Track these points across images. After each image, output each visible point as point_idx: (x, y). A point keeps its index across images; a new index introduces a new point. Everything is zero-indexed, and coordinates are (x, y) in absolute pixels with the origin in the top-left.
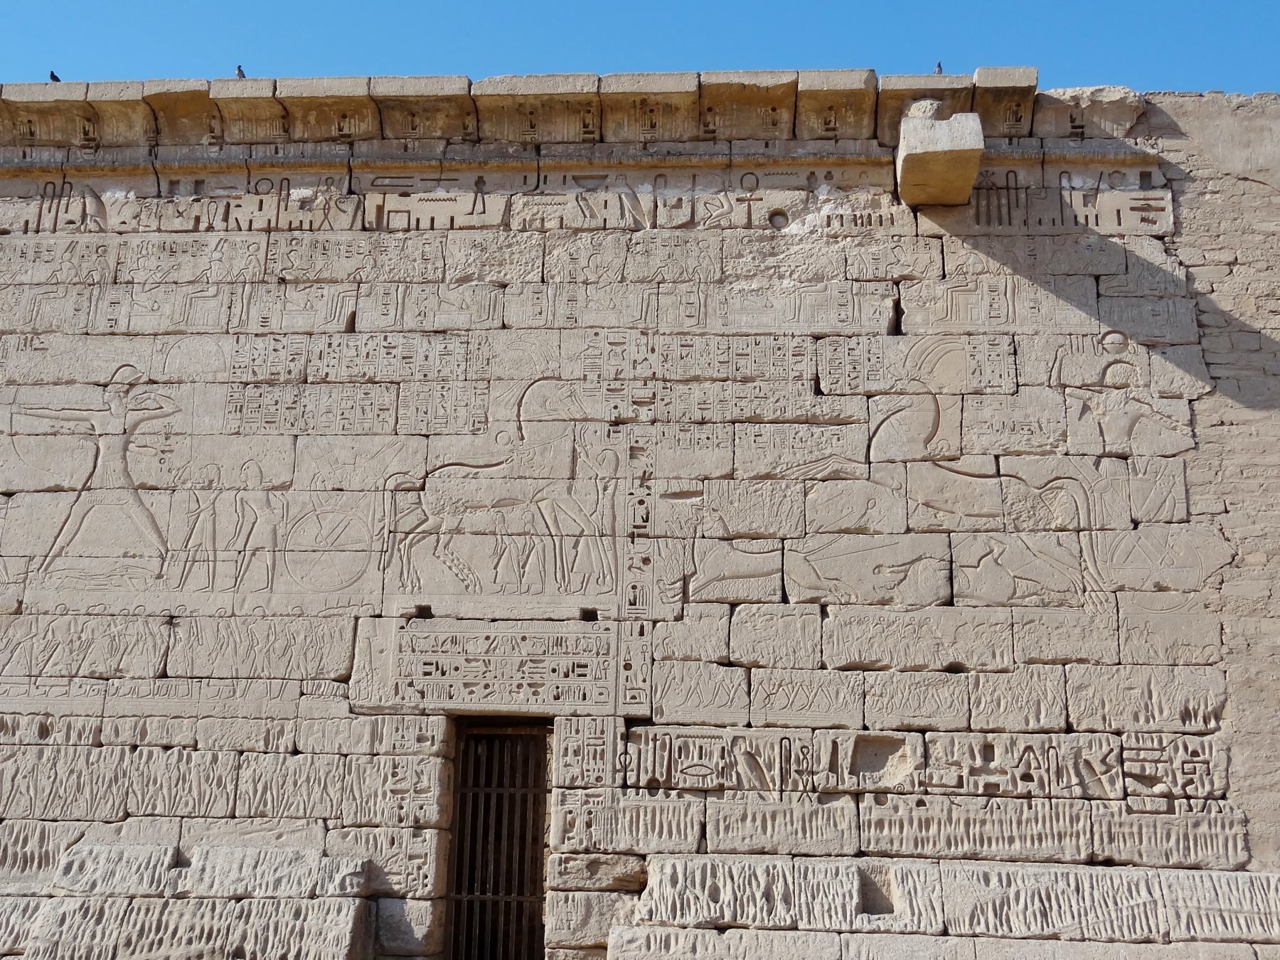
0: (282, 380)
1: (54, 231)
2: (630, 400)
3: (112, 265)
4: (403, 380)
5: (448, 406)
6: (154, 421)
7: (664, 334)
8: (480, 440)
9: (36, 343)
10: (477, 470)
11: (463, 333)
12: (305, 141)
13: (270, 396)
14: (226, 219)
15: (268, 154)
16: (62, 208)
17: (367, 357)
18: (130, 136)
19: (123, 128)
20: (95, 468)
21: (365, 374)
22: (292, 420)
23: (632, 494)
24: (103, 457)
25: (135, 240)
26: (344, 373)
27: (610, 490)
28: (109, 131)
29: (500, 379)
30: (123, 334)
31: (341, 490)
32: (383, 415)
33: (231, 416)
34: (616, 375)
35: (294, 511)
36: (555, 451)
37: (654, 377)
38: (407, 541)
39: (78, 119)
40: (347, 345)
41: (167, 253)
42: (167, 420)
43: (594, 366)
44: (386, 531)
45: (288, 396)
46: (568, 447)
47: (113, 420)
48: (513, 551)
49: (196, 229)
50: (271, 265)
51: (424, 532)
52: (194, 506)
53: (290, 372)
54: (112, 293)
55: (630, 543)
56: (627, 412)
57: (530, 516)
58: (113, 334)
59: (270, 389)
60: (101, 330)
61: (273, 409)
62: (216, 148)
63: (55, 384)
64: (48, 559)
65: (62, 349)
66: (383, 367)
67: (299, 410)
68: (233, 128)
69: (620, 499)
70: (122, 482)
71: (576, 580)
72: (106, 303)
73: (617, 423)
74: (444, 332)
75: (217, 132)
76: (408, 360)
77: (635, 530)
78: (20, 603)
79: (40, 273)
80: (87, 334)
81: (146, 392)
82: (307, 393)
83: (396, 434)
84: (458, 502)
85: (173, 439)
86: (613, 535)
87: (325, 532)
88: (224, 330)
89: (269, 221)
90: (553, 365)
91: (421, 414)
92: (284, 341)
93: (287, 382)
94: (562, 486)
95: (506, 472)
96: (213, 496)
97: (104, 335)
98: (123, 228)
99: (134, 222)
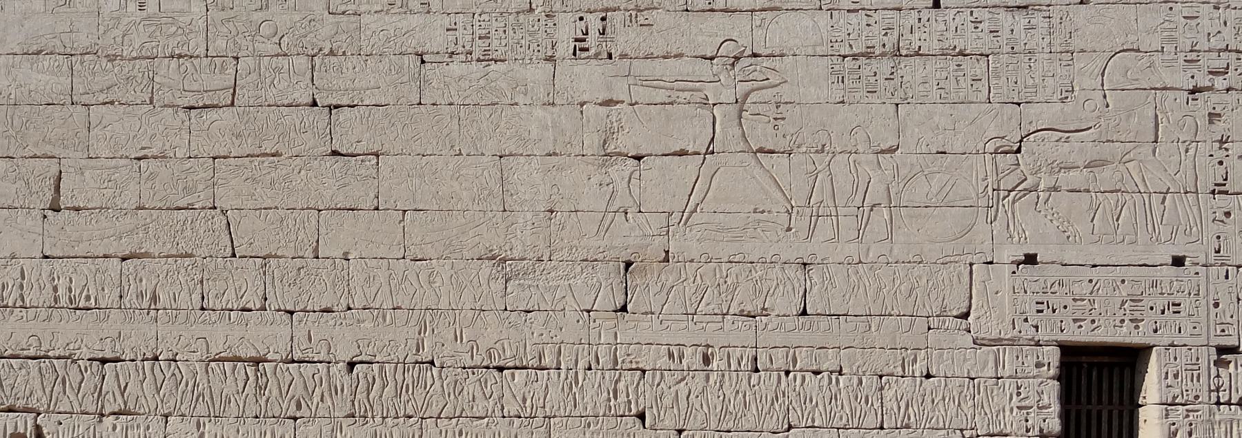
0: (877, 53)
2: (1206, 70)
4: (992, 53)
5: (1036, 75)
6: (764, 91)
7: (1235, 8)
8: (1068, 107)
9: (641, 20)
10: (1067, 135)
11: (1045, 8)
17: (956, 31)
20: (714, 133)
21: (955, 47)
22: (892, 90)
23: (1212, 156)
24: (721, 125)
26: (935, 47)
27: (1191, 152)
29: (1083, 51)
30: (721, 11)
31: (945, 153)
32: (976, 85)
34: (1192, 47)
35: (903, 172)
36: (1139, 118)
37: (1227, 49)
38: (1011, 198)
40: (936, 20)
43: (1172, 39)
44: (990, 189)
45: (885, 67)
46: (1151, 114)
47: (724, 91)
48: (1107, 206)
51: (1025, 190)
52: (811, 168)
53: (884, 45)
55: (1212, 199)
56: (1204, 81)
57: (1120, 176)
58: (712, 10)
59: (868, 61)
60: (700, 7)
61: (872, 80)
63: (665, 57)
64: (686, 216)
65: (666, 25)
66: (969, 41)
67: (897, 81)
69: (1202, 160)
70: (742, 146)
71: (1165, 233)
73: (1193, 92)
74: (1026, 7)
76: (995, 34)
77: (1216, 187)
80: (687, 10)
81: (751, 65)
82: (902, 65)
83: (990, 102)
84: (1053, 163)
86: (1197, 192)
87: (934, 190)
88: (818, 7)
90: (1132, 38)
91: (1011, 84)
92: (876, 16)
93: (883, 55)
94: (1148, 148)
95: (1095, 137)
96: (828, 159)
97: (703, 11)
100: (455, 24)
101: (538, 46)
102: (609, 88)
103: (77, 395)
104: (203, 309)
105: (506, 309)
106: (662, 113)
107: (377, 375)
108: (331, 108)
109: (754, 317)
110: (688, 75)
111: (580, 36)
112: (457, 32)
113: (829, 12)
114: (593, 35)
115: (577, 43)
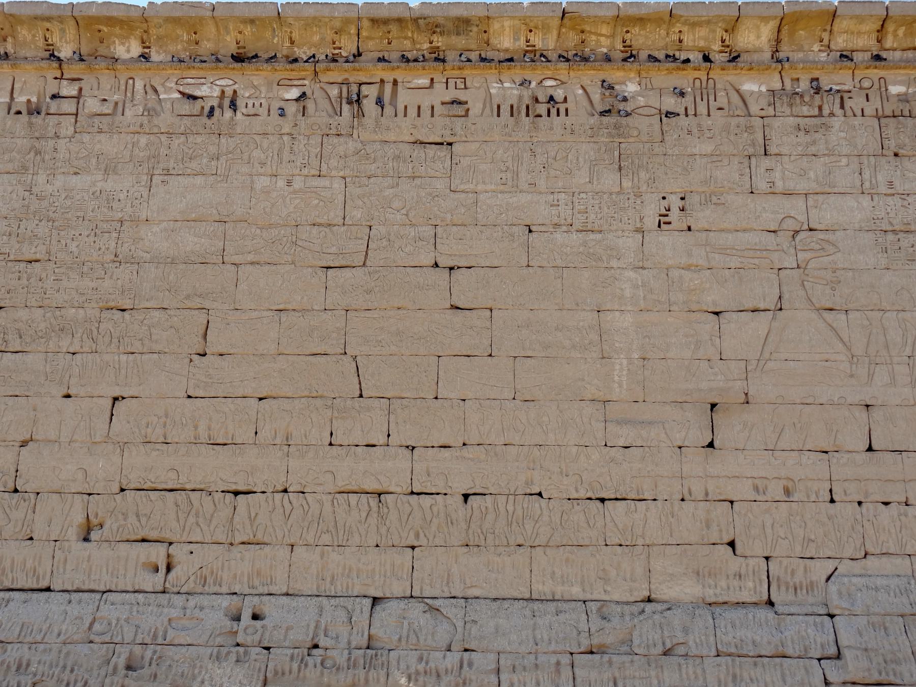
1: (709, 115)
3: (761, 141)
12: (894, 50)
13: (907, 241)
14: (842, 107)
15: (866, 59)
16: (712, 98)
18: (757, 43)
19: (752, 37)
25: (777, 123)
28: (742, 39)
33: (880, 256)
39: (718, 30)
41: (802, 133)
42: (830, 258)
49: (821, 115)
50: (886, 142)
54: (766, 162)
62: (825, 54)
68: (838, 39)
72: (763, 170)
75: (826, 42)
78: (746, 394)
79: (708, 148)
85: (838, 273)
89: (877, 110)
92: (910, 199)
98: (763, 113)
99: (771, 109)
100: (558, 201)
101: (629, 219)
102: (690, 255)
103: (209, 526)
104: (331, 444)
105: (606, 445)
106: (736, 276)
107: (490, 506)
108: (451, 269)
109: (826, 452)
110: (756, 244)
111: (664, 212)
112: (560, 208)
113: (870, 195)
114: (675, 211)
115: (661, 218)
